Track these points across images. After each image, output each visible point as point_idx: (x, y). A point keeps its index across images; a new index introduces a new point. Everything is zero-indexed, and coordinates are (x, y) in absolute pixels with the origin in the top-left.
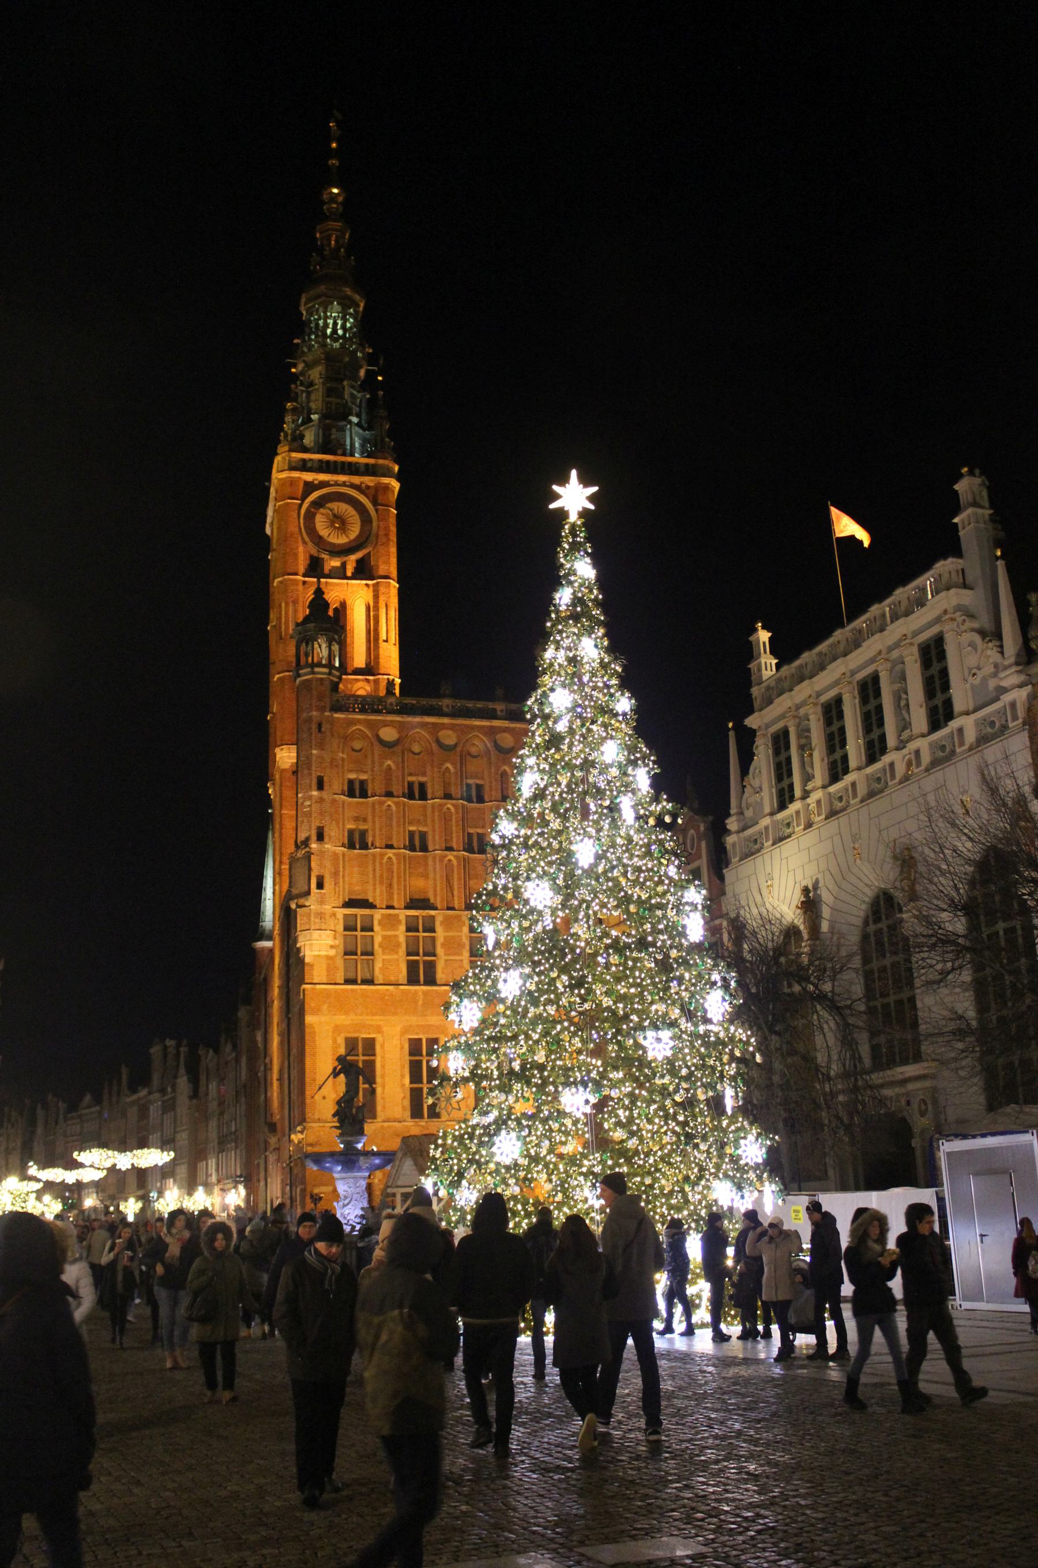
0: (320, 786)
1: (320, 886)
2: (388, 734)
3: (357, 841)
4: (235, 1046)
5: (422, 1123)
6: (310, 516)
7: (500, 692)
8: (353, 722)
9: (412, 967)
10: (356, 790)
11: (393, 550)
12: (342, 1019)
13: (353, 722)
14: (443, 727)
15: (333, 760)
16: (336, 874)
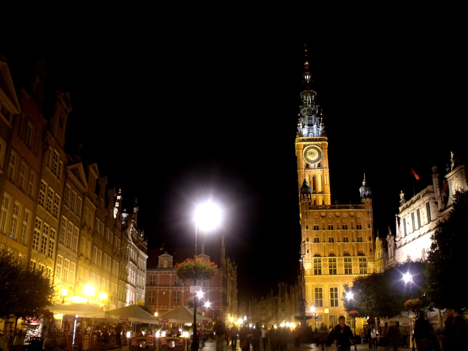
0: (307, 228)
1: (308, 252)
2: (323, 214)
3: (317, 240)
4: (298, 286)
5: (333, 308)
6: (305, 154)
7: (350, 202)
8: (314, 212)
9: (331, 271)
10: (316, 228)
11: (327, 160)
12: (314, 283)
13: (314, 212)
14: (337, 212)
15: (310, 222)
16: (312, 249)
